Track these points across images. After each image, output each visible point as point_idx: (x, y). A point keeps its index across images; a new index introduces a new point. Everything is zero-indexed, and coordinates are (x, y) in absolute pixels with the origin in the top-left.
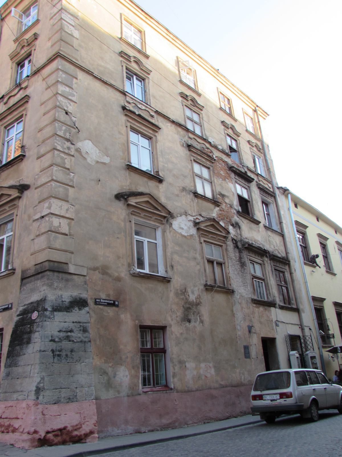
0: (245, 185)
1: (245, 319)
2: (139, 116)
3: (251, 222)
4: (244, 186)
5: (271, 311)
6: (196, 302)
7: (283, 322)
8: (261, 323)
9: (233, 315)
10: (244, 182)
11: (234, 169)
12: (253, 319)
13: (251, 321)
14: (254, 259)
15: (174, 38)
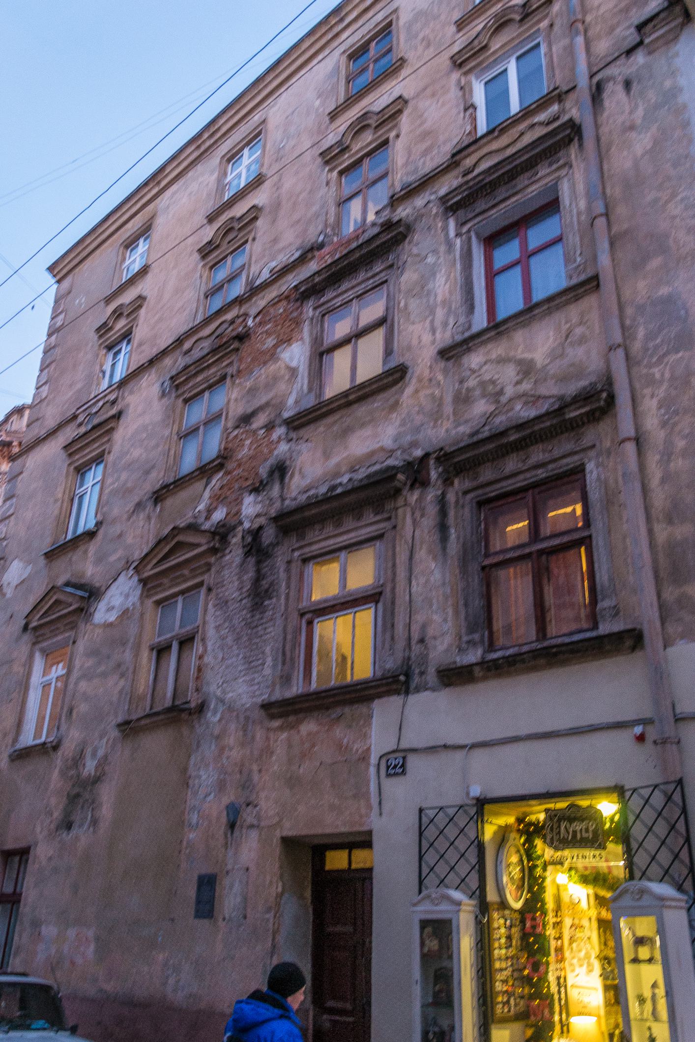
0: (371, 281)
1: (221, 786)
2: (94, 428)
3: (356, 406)
4: (360, 289)
5: (371, 716)
6: (95, 776)
7: (445, 747)
8: (292, 781)
9: (185, 782)
10: (354, 282)
11: (303, 289)
12: (256, 777)
13: (246, 785)
14: (331, 542)
15: (212, 130)
